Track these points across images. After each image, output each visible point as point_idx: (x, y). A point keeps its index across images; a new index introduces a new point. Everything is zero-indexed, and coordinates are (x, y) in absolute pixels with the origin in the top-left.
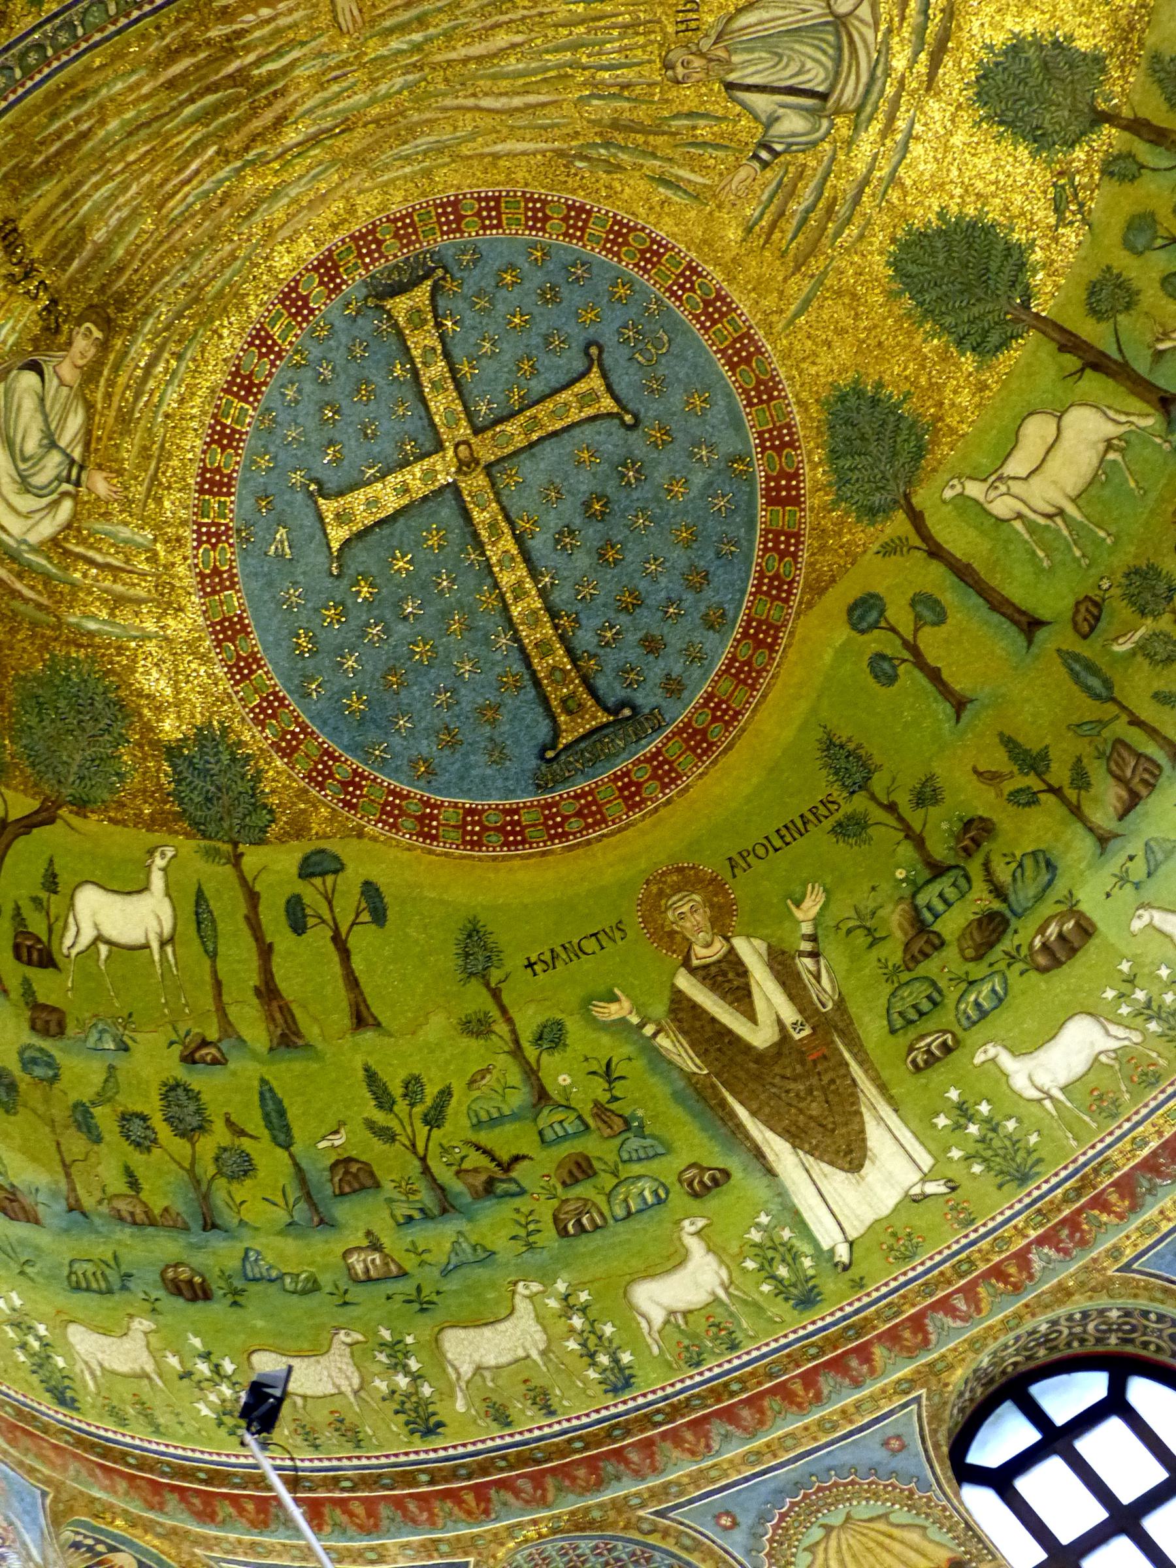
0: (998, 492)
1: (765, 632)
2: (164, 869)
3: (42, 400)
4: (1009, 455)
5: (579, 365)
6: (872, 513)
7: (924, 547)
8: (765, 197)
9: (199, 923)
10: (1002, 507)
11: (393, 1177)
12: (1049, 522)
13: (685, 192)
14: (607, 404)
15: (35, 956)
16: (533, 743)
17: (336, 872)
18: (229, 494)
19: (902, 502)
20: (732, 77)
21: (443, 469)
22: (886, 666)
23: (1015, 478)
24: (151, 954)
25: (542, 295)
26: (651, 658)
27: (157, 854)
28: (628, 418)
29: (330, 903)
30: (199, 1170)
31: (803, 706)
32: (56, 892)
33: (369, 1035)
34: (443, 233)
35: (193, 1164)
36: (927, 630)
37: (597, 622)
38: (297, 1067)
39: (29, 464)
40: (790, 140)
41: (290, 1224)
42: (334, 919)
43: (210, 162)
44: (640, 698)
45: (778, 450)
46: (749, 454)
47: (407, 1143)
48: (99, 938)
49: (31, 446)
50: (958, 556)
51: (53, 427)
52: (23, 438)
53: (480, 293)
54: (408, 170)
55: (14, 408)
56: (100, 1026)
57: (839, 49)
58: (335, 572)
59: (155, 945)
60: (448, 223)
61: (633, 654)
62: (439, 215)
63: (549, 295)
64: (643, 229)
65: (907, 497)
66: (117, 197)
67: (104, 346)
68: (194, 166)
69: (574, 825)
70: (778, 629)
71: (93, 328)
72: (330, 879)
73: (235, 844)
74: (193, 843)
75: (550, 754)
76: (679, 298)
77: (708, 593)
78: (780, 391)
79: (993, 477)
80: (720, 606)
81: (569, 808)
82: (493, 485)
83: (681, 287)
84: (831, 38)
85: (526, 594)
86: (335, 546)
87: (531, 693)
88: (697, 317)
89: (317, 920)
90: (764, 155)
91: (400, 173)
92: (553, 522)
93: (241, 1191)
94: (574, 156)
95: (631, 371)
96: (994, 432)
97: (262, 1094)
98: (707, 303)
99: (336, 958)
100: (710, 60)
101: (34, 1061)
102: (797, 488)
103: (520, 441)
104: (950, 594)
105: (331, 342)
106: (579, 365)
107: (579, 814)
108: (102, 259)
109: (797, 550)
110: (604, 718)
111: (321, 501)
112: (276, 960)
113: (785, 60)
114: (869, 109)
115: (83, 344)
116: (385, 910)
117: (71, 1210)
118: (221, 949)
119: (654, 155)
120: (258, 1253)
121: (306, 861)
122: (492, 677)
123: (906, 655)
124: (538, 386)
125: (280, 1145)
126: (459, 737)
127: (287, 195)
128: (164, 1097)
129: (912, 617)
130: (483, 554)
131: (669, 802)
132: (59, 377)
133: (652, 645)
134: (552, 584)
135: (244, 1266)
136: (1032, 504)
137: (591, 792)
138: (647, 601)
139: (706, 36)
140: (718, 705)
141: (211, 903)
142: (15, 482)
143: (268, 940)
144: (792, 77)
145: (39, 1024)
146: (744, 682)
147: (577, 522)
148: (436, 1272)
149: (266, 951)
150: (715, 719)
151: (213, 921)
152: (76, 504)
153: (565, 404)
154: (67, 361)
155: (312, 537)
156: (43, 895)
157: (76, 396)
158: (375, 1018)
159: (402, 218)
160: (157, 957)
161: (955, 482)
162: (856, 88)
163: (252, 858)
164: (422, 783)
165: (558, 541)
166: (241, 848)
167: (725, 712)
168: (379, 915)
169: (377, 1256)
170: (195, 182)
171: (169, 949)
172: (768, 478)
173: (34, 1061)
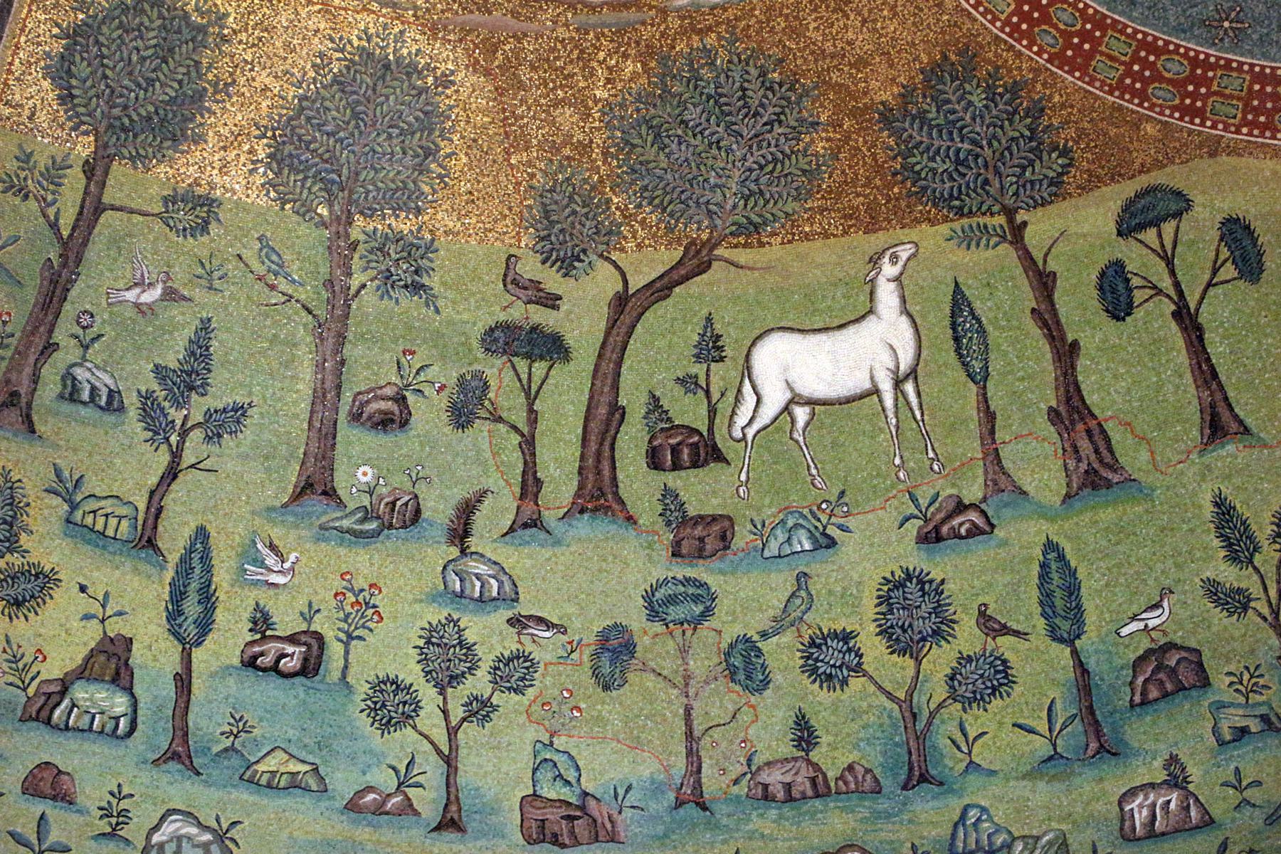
9: (957, 339)
11: (1232, 668)
15: (686, 454)
17: (1178, 215)
24: (881, 401)
27: (886, 260)
29: (1169, 263)
30: (919, 699)
32: (722, 359)
33: (1229, 449)
35: (910, 694)
38: (1107, 515)
41: (1050, 758)
42: (1177, 285)
47: (1266, 611)
48: (796, 399)
56: (790, 523)
59: (886, 386)
72: (1168, 228)
74: (944, 229)
93: (977, 721)
97: (1044, 566)
99: (1178, 339)
101: (672, 600)
112: (1082, 363)
116: (1260, 254)
117: (680, 803)
118: (995, 366)
120: (984, 810)
121: (1128, 207)
125: (1061, 640)
128: (884, 600)
135: (954, 836)
141: (977, 305)
143: (1070, 338)
148: (1258, 817)
149: (1066, 353)
151: (982, 331)
156: (699, 370)
158: (1241, 422)
160: (889, 402)
166: (1021, 216)
169: (1174, 797)
171: (909, 388)
173: (672, 600)
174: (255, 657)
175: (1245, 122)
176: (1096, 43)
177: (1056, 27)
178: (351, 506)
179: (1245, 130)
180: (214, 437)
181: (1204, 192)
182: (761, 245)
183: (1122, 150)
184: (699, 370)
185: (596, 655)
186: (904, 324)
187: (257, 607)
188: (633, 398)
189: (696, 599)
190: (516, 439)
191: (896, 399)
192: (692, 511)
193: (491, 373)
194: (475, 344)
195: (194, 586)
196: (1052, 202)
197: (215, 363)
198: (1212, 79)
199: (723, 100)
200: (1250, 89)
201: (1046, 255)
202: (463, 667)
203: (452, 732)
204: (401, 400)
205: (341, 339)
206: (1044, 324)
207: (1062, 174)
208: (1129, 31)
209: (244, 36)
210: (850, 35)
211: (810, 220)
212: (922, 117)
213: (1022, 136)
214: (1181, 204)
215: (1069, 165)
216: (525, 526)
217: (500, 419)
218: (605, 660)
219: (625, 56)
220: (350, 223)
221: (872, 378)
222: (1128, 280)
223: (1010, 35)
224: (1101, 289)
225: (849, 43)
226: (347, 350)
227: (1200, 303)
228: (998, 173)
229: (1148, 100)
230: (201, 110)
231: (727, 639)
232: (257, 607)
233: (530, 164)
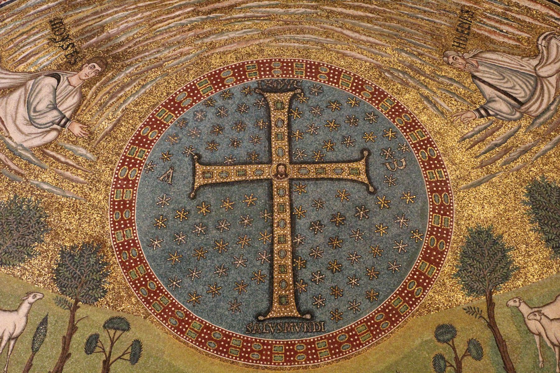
0: (535, 318)
1: (393, 314)
2: (31, 304)
4: (548, 304)
5: (356, 155)
6: (470, 290)
7: (488, 320)
8: (476, 129)
10: (533, 325)
12: (552, 347)
13: (437, 109)
14: (363, 177)
16: (257, 309)
17: (124, 330)
18: (148, 148)
19: (488, 294)
20: (476, 74)
21: (268, 172)
22: (442, 363)
23: (546, 316)
25: (349, 119)
26: (333, 297)
27: (32, 295)
28: (371, 189)
31: (393, 358)
34: (306, 75)
36: (470, 358)
37: (316, 269)
39: (37, 114)
40: (498, 113)
42: (110, 352)
43: (189, 12)
44: (318, 313)
45: (438, 239)
46: (423, 232)
49: (41, 107)
50: (502, 333)
51: (57, 101)
52: (38, 103)
53: (317, 106)
54: (296, 45)
55: (37, 91)
57: (535, 89)
58: (191, 196)
59: (6, 338)
60: (311, 72)
61: (325, 292)
62: (307, 68)
63: (353, 121)
64: (410, 114)
65: (491, 294)
67: (101, 74)
68: (177, 13)
69: (255, 356)
70: (400, 316)
72: (119, 333)
73: (77, 301)
75: (261, 318)
76: (418, 150)
77: (375, 282)
78: (450, 213)
79: (536, 310)
80: (378, 291)
81: (257, 347)
82: (290, 188)
83: (420, 146)
84: (532, 83)
85: (286, 242)
86: (197, 185)
87: (266, 286)
88: (423, 162)
89: (101, 350)
90: (483, 112)
91: (292, 44)
92: (313, 216)
94: (386, 70)
95: (382, 169)
96: (546, 290)
98: (430, 158)
100: (467, 63)
102: (440, 260)
103: (312, 175)
104: (489, 349)
105: (230, 101)
106: (356, 155)
107: (260, 352)
108: (110, 40)
109: (427, 286)
110: (296, 313)
111: (197, 164)
112: (68, 362)
113: (506, 80)
114: (542, 120)
115: (87, 72)
118: (42, 349)
119: (426, 87)
121: (111, 320)
122: (251, 271)
123: (455, 365)
124: (330, 156)
126: (221, 292)
127: (227, 35)
129: (466, 348)
130: (272, 216)
131: (306, 368)
132: (69, 82)
133: (336, 292)
134: (300, 243)
136: (548, 333)
137: (271, 345)
138: (344, 271)
139: (468, 53)
140: (353, 336)
141: (49, 325)
142: (26, 120)
144: (507, 88)
146: (372, 332)
147: (326, 222)
149: (65, 356)
150: (348, 341)
151: (45, 335)
152: (59, 134)
153: (342, 169)
154: (76, 76)
155: (185, 178)
159: (287, 63)
161: (517, 300)
162: (540, 107)
163: (83, 311)
164: (189, 305)
165: (311, 226)
167: (355, 340)
168: (135, 357)
170: (176, 19)
171: (12, 342)
172: (428, 248)
175: (160, 314)
176: (136, 265)
177: (129, 254)
179: (159, 316)
181: (135, 328)
183: (121, 301)
186: (24, 319)
191: (6, 344)
196: (91, 305)
198: (160, 296)
200: (168, 306)
201: (79, 321)
206: (64, 343)
207: (99, 297)
208: (148, 268)
213: (96, 280)
214: (126, 327)
215: (104, 297)
221: (3, 333)
222: (97, 342)
223: (116, 248)
224: (88, 341)
225: (70, 223)
227: (113, 362)
228: (82, 286)
229: (139, 291)
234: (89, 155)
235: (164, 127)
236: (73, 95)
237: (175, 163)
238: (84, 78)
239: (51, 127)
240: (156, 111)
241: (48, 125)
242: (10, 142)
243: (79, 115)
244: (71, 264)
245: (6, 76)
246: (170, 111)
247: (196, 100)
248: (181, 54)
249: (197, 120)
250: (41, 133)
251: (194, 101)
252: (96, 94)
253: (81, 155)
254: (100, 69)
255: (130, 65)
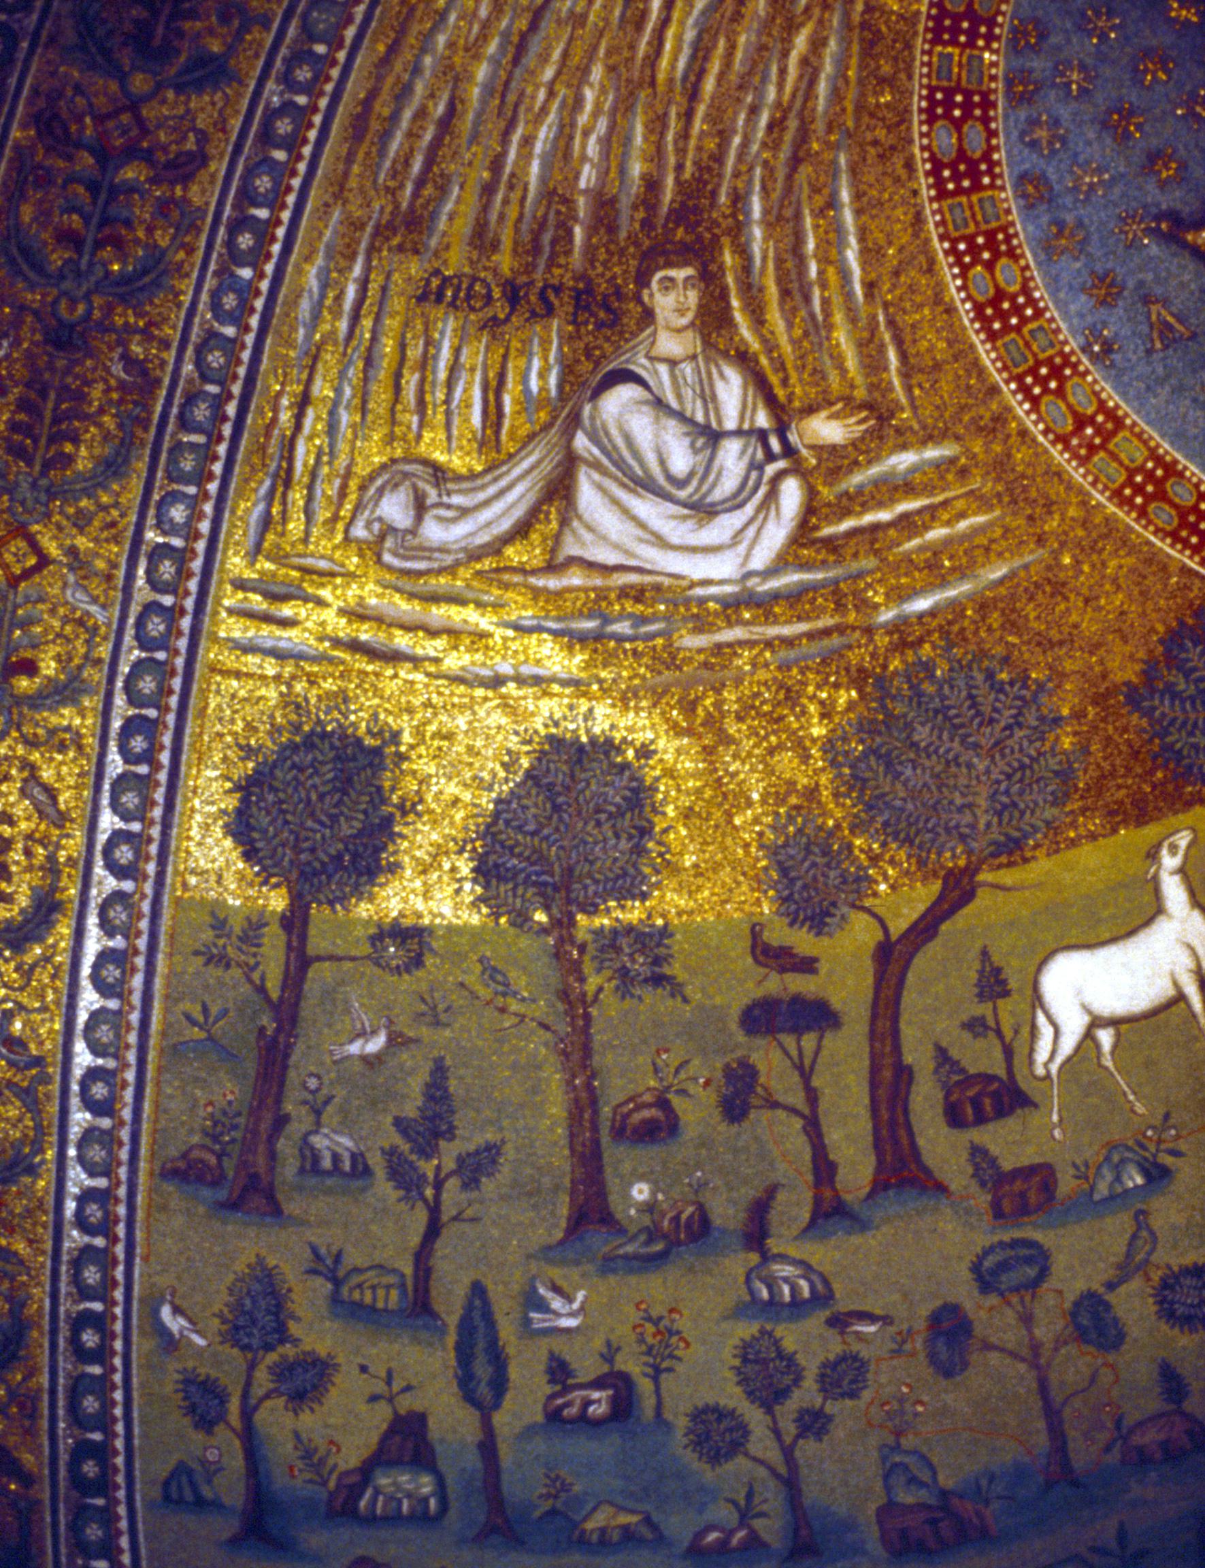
3: (659, 403)
27: (1165, 852)
32: (1006, 993)
39: (695, 483)
48: (1096, 1022)
49: (681, 460)
51: (700, 417)
55: (620, 442)
56: (1116, 1158)
66: (573, 125)
67: (709, 278)
71: (673, 273)
105: (1054, 40)
142: (684, 518)
145: (1007, 1205)
156: (985, 1009)
157: (708, 360)
173: (1003, 1266)
174: (560, 1409)
178: (633, 1229)
180: (471, 1185)
182: (1026, 860)
184: (985, 1009)
185: (930, 1342)
187: (553, 1357)
188: (916, 1054)
189: (1028, 1260)
190: (798, 1123)
192: (1007, 1165)
193: (756, 1058)
194: (734, 1026)
195: (481, 1344)
197: (456, 1104)
199: (953, 712)
202: (788, 1380)
203: (788, 1453)
204: (663, 1103)
205: (587, 1050)
209: (422, 750)
210: (1074, 618)
211: (1073, 825)
212: (1171, 691)
216: (827, 1216)
217: (775, 1105)
218: (941, 1346)
219: (836, 686)
220: (572, 923)
225: (1076, 626)
226: (596, 1060)
230: (393, 836)
231: (1070, 1298)
232: (553, 1357)
233: (756, 821)
234: (932, 453)
235: (1008, 239)
236: (715, 375)
237: (1141, 284)
238: (684, 321)
239: (766, 478)
240: (943, 222)
241: (751, 483)
242: (713, 590)
243: (790, 398)
244: (1184, 709)
245: (503, 483)
246: (968, 192)
247: (985, 112)
248: (804, 62)
249: (1053, 152)
250: (758, 511)
251: (986, 120)
252: (758, 321)
253: (914, 469)
254: (689, 271)
255: (739, 199)
